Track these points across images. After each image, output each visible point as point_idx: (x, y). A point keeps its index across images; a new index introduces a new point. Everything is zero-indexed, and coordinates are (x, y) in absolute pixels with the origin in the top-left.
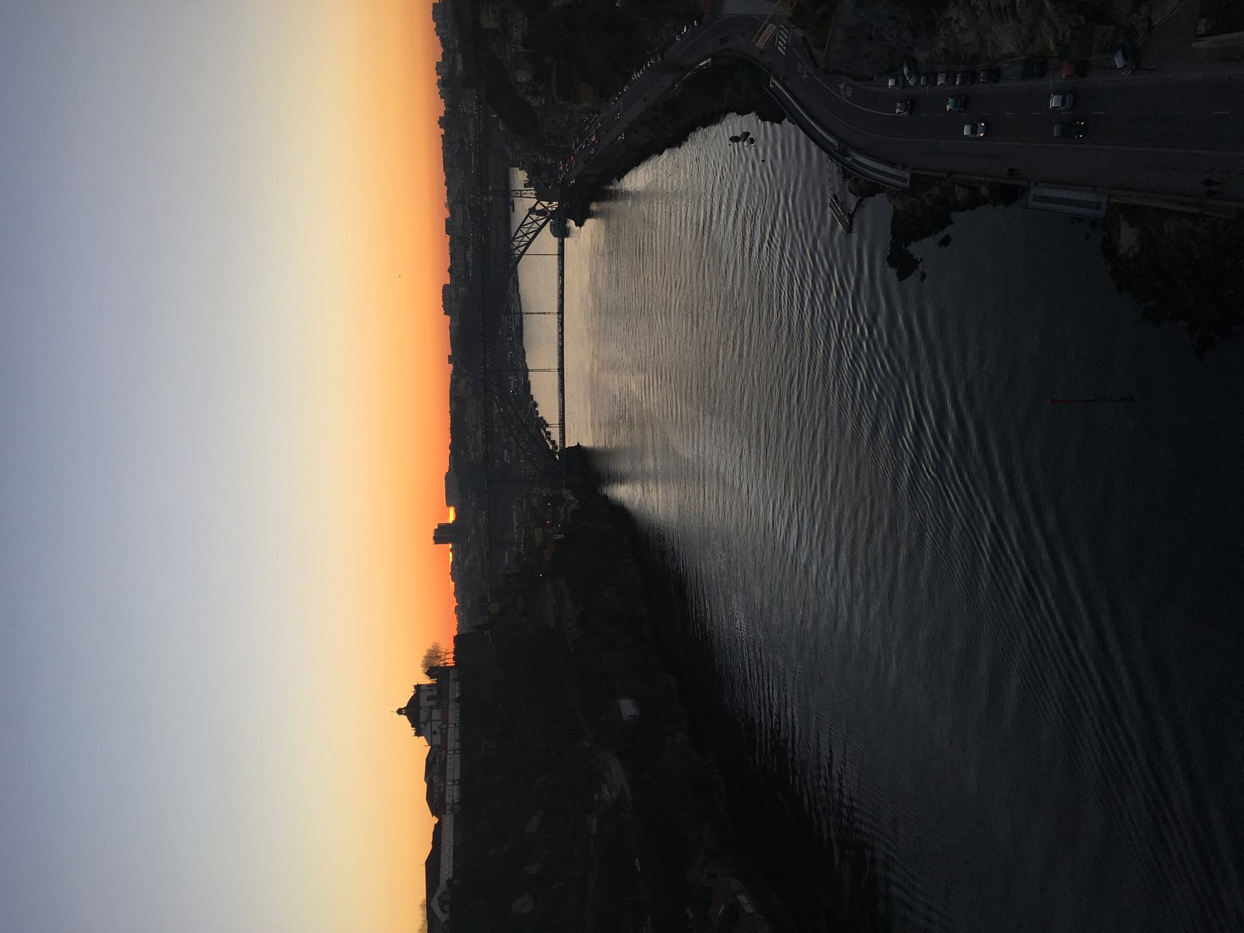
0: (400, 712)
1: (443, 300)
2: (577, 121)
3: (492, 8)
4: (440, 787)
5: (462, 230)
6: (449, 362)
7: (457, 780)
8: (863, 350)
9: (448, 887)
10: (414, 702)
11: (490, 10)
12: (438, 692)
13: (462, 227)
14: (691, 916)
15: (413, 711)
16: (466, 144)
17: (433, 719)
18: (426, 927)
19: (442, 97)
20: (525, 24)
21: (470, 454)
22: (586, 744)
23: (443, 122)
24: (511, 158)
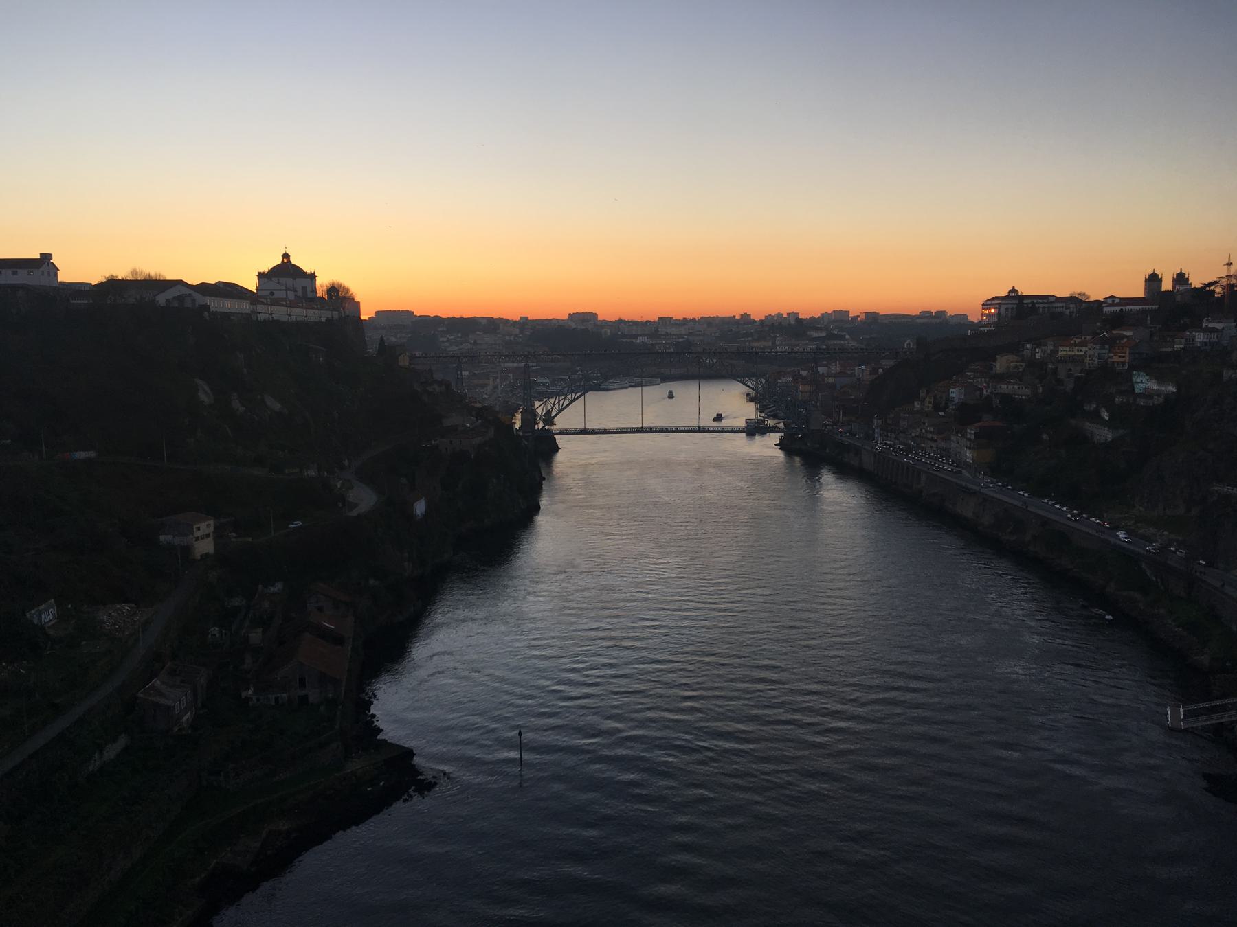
0: (286, 256)
1: (583, 313)
2: (923, 445)
3: (1021, 366)
5: (663, 333)
6: (521, 318)
7: (273, 318)
8: (619, 731)
9: (201, 306)
10: (297, 272)
11: (1018, 364)
13: (667, 333)
14: (272, 589)
15: (286, 271)
16: (746, 339)
18: (162, 279)
19: (766, 317)
20: (1017, 396)
22: (346, 463)
23: (745, 317)
24: (779, 381)
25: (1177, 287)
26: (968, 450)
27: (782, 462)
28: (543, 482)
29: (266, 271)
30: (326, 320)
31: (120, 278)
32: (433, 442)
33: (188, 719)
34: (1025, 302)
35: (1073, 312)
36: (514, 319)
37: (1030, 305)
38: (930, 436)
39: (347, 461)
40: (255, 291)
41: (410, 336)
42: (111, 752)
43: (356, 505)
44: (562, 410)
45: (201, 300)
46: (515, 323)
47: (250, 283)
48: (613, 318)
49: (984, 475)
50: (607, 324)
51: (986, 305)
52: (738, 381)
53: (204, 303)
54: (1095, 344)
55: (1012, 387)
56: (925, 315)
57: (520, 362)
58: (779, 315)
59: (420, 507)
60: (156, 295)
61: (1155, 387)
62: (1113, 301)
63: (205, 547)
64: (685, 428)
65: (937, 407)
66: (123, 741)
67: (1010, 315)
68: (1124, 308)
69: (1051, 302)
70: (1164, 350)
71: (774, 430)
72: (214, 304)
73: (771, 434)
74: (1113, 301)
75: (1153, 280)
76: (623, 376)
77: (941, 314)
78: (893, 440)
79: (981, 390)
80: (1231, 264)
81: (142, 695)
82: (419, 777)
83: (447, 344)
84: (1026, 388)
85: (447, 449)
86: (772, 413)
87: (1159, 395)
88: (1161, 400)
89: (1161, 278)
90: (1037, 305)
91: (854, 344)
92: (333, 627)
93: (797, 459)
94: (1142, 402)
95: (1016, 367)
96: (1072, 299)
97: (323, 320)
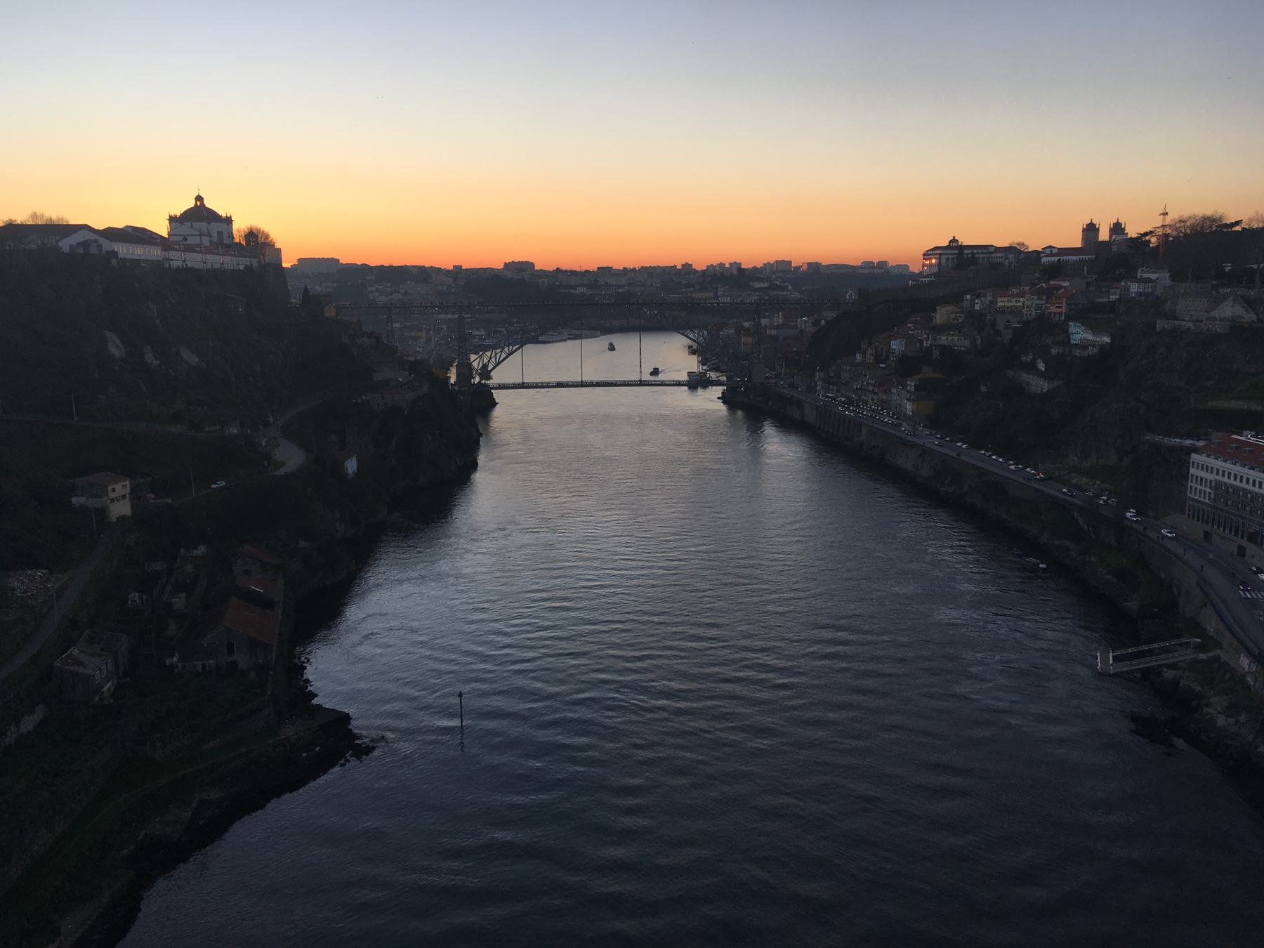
0: (199, 198)
1: (519, 262)
2: (864, 397)
3: (961, 317)
4: (180, 245)
5: (604, 284)
10: (212, 216)
11: (958, 315)
12: (226, 244)
13: (606, 283)
14: (195, 552)
15: (200, 215)
17: (203, 237)
18: (65, 223)
20: (956, 348)
21: (373, 287)
22: (271, 419)
23: (687, 266)
24: (721, 333)
25: (1114, 237)
26: (908, 404)
27: (726, 416)
28: (481, 439)
29: (178, 214)
30: (245, 268)
31: (19, 222)
32: (364, 397)
33: (109, 689)
34: (965, 252)
35: (1012, 263)
36: (447, 268)
37: (970, 256)
38: (871, 388)
39: (271, 417)
40: (167, 236)
41: (336, 285)
42: (28, 724)
43: (283, 464)
44: (499, 363)
45: (108, 245)
46: (447, 273)
47: (161, 228)
48: (552, 268)
49: (923, 427)
50: (544, 273)
51: (927, 255)
52: (680, 333)
53: (110, 249)
54: (1033, 294)
55: (951, 338)
56: (868, 265)
57: (453, 313)
58: (721, 265)
59: (351, 466)
60: (59, 241)
61: (1091, 337)
62: (1051, 251)
63: (121, 509)
64: (624, 381)
65: (878, 359)
66: (39, 713)
67: (950, 265)
68: (1061, 258)
69: (991, 253)
70: (1098, 300)
71: (719, 383)
72: (123, 250)
73: (714, 387)
74: (1051, 251)
75: (1091, 229)
76: (562, 329)
77: (882, 264)
78: (834, 392)
79: (921, 342)
80: (1167, 213)
81: (59, 664)
82: (356, 742)
83: (377, 294)
84: (965, 339)
85: (378, 405)
86: (714, 366)
87: (1094, 346)
88: (1096, 350)
89: (1098, 230)
90: (977, 256)
91: (796, 295)
92: (262, 591)
93: (740, 413)
94: (1077, 352)
95: (956, 318)
96: (1011, 249)
97: (242, 267)
